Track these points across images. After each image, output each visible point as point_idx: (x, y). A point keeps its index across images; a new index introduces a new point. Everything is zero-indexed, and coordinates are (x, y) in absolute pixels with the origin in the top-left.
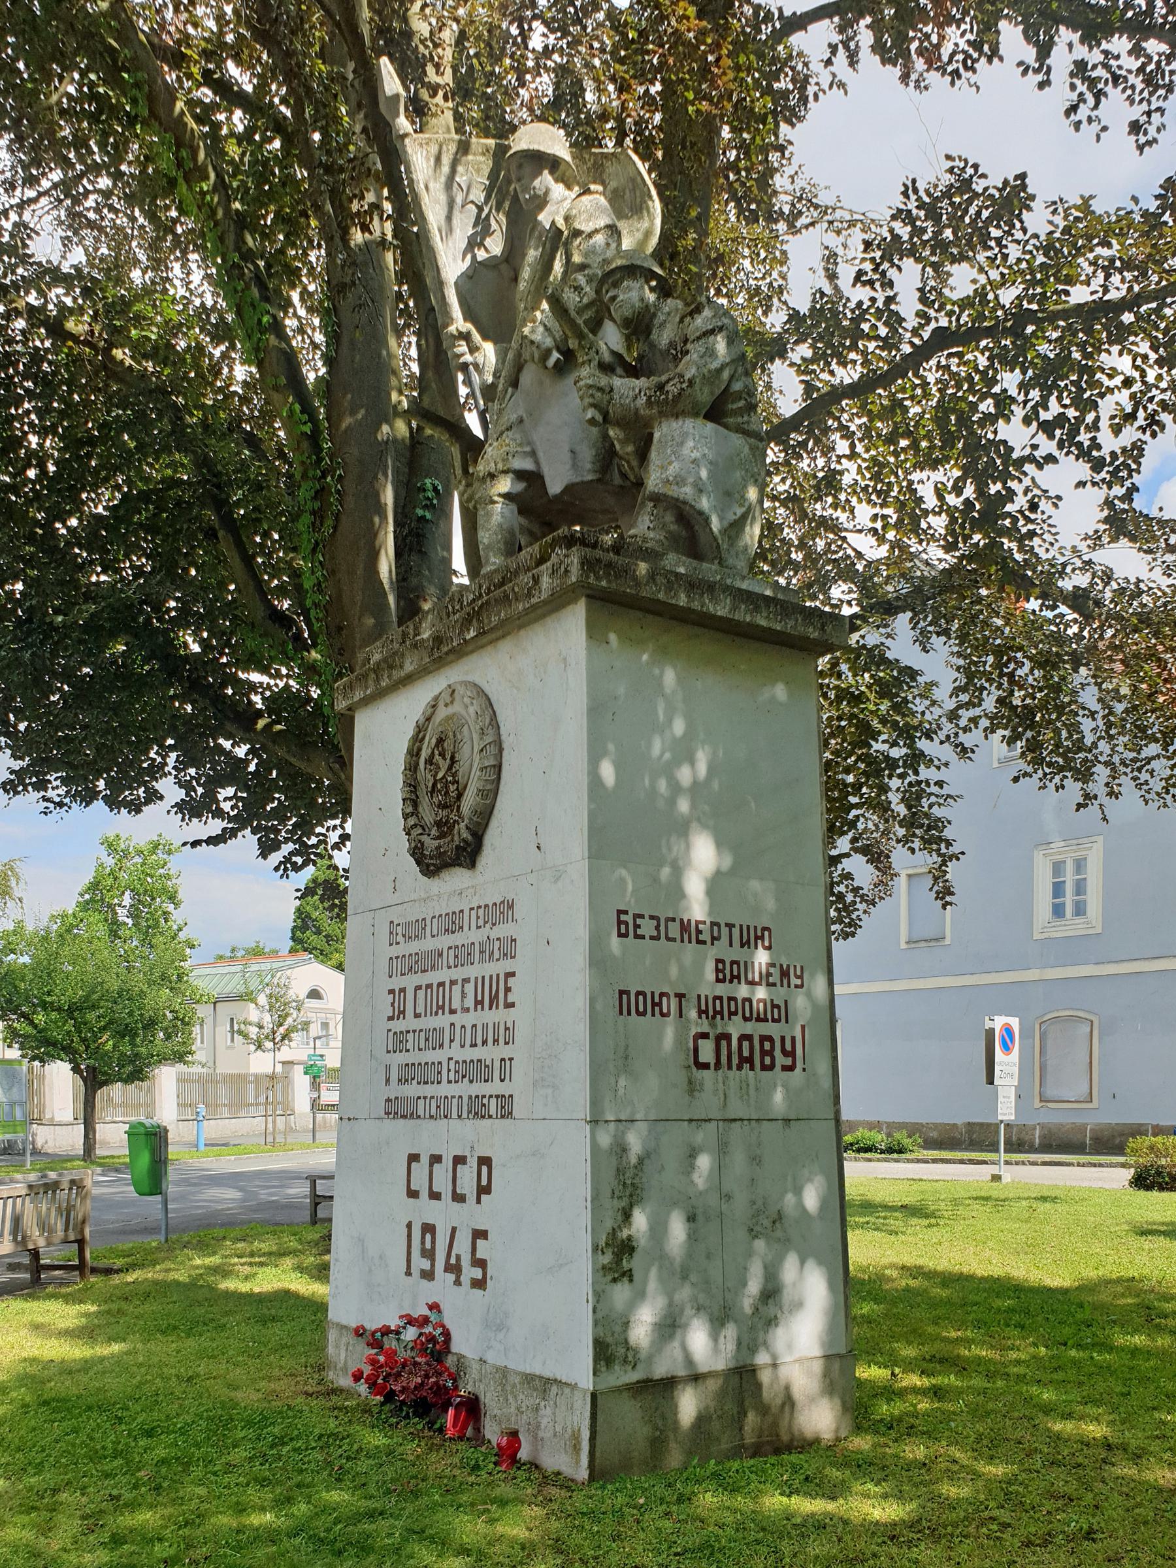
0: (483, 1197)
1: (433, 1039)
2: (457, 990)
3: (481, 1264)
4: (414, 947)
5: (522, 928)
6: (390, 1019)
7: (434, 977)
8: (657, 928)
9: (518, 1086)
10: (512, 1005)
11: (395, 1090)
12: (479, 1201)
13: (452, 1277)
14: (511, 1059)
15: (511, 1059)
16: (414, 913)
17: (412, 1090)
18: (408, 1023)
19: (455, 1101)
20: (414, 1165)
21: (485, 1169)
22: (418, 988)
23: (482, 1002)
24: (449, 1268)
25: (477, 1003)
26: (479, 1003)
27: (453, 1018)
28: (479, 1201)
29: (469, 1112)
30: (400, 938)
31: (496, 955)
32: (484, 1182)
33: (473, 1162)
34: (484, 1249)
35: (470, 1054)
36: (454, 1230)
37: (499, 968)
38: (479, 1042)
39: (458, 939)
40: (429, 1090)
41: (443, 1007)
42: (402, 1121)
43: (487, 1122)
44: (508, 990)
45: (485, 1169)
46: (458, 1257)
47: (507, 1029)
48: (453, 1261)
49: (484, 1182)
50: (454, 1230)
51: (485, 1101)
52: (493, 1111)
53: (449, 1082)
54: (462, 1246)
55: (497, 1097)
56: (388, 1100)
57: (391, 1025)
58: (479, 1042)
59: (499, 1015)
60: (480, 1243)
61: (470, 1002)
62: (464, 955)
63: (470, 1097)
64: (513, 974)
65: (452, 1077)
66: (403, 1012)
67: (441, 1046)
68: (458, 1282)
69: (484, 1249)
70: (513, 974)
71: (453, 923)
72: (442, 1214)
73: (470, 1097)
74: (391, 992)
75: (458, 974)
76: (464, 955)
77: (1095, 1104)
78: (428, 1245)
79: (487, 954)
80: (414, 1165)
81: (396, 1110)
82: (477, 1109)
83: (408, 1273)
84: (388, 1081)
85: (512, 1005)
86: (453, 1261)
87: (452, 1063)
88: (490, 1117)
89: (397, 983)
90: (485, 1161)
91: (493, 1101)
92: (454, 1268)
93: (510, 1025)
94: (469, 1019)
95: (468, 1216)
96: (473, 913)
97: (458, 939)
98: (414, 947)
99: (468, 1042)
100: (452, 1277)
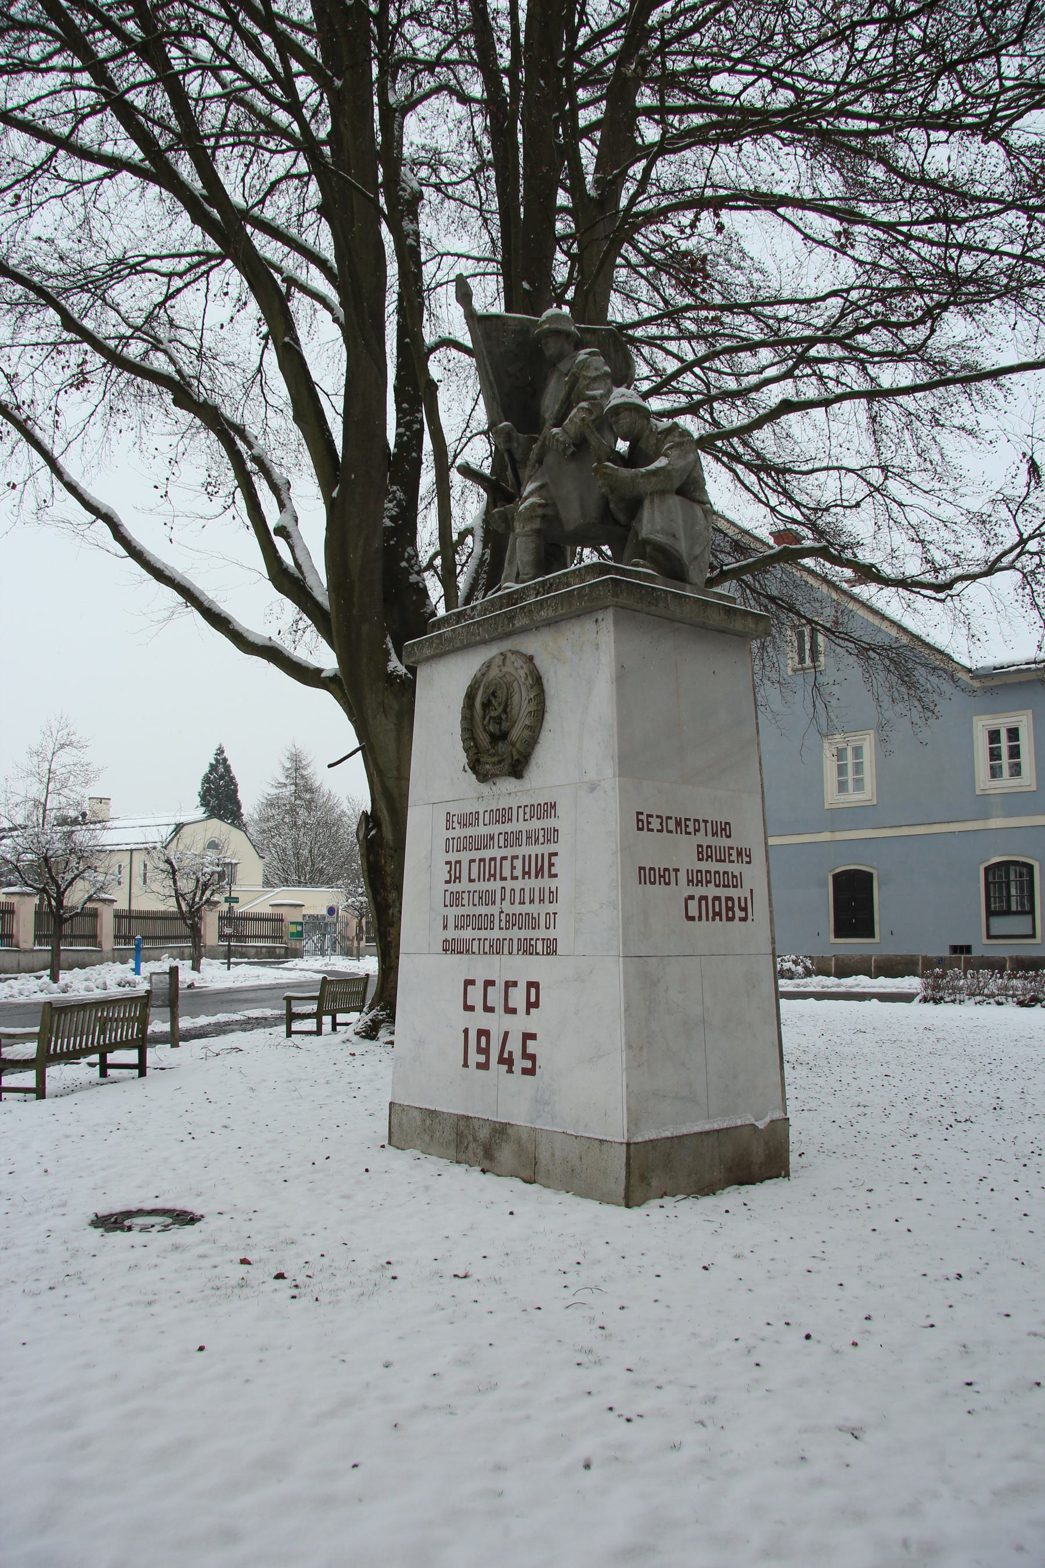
0: (532, 1010)
1: (485, 897)
2: (507, 864)
3: (532, 1058)
4: (470, 831)
5: (562, 822)
6: (447, 882)
7: (487, 854)
8: (661, 824)
9: (560, 932)
10: (556, 876)
11: (451, 934)
12: (528, 1013)
13: (506, 1067)
14: (555, 914)
15: (555, 914)
17: (468, 934)
18: (464, 885)
19: (506, 943)
21: (533, 991)
22: (472, 861)
23: (529, 873)
24: (501, 1061)
25: (524, 873)
26: (526, 873)
27: (503, 883)
28: (528, 1013)
29: (519, 950)
30: (456, 825)
31: (541, 840)
32: (533, 999)
33: (522, 986)
34: (532, 1047)
35: (518, 909)
36: (506, 1034)
37: (546, 849)
38: (527, 900)
39: (508, 827)
40: (483, 934)
41: (494, 876)
42: (460, 955)
43: (534, 957)
44: (551, 865)
45: (533, 991)
46: (510, 1053)
47: (551, 892)
48: (506, 1055)
49: (533, 999)
50: (506, 1034)
52: (539, 949)
53: (501, 929)
54: (514, 1045)
55: (543, 940)
56: (446, 941)
57: (448, 886)
58: (527, 900)
59: (545, 882)
60: (529, 1042)
61: (518, 872)
62: (512, 839)
63: (519, 939)
64: (556, 854)
65: (503, 925)
66: (459, 878)
67: (494, 903)
68: (510, 1071)
69: (532, 1047)
70: (556, 854)
71: (503, 816)
72: (496, 1023)
73: (519, 939)
74: (447, 863)
75: (509, 852)
76: (512, 839)
77: (1038, 940)
78: (483, 1044)
79: (532, 838)
80: (470, 987)
81: (450, 947)
82: (527, 948)
83: (466, 1065)
84: (445, 927)
85: (556, 876)
86: (506, 1055)
87: (503, 916)
88: (537, 954)
89: (453, 857)
90: (533, 985)
91: (540, 943)
92: (507, 1061)
93: (553, 889)
94: (517, 885)
95: (518, 1024)
96: (521, 811)
97: (508, 827)
98: (470, 831)
99: (517, 900)
100: (506, 1067)
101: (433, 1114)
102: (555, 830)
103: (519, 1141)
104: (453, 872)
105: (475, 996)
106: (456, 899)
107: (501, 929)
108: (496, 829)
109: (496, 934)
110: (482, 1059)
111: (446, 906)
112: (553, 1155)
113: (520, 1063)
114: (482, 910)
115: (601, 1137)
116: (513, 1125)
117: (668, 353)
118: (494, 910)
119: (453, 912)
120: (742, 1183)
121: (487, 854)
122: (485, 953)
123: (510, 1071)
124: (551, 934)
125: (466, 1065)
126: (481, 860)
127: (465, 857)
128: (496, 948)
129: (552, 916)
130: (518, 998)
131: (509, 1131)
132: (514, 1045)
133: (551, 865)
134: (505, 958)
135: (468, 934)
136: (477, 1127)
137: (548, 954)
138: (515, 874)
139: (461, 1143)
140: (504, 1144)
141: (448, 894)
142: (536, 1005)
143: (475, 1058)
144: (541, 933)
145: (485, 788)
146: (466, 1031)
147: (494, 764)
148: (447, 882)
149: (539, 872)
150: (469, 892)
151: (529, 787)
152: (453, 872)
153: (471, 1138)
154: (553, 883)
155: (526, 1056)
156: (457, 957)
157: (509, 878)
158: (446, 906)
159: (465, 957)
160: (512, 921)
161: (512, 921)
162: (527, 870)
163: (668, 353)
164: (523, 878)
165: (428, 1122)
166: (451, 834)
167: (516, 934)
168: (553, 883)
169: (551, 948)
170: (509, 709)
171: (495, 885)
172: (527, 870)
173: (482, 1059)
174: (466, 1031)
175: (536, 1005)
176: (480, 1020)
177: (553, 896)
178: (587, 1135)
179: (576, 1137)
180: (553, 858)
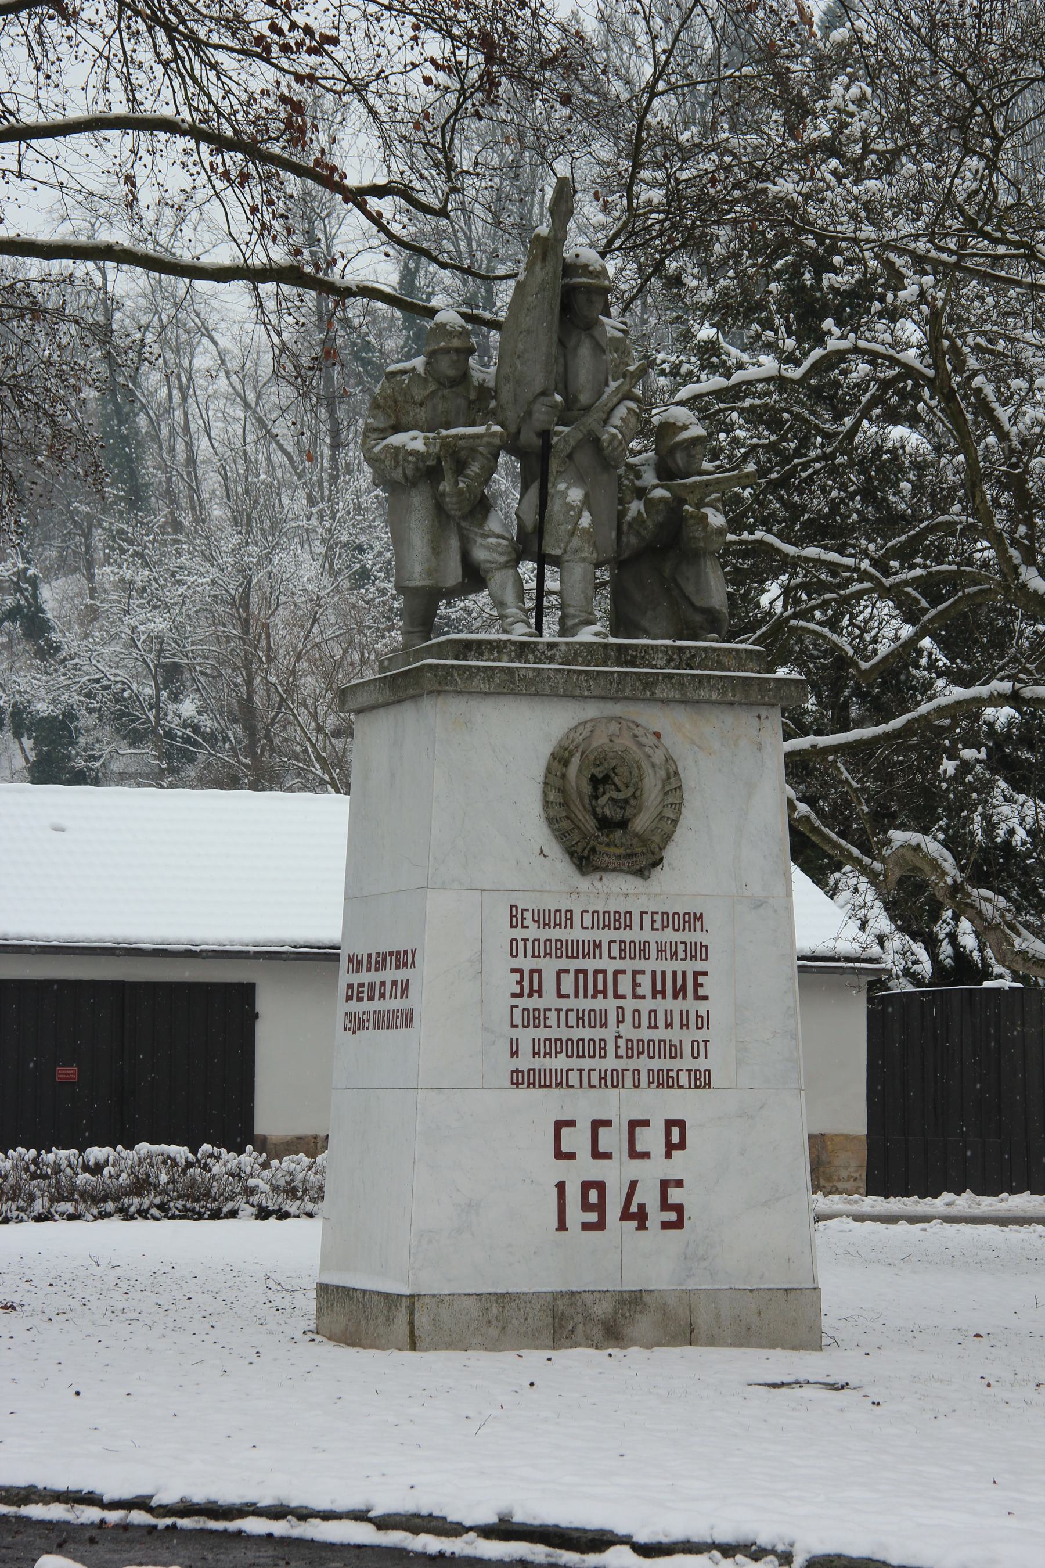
3: (679, 1209)
4: (555, 934)
5: (714, 935)
6: (514, 995)
7: (590, 965)
9: (715, 1062)
11: (525, 1061)
12: (668, 1155)
13: (635, 1223)
14: (706, 1042)
15: (706, 1042)
16: (551, 904)
17: (560, 1062)
20: (565, 1131)
24: (626, 1216)
27: (620, 1002)
28: (668, 1155)
29: (649, 1083)
30: (528, 922)
31: (681, 955)
36: (633, 1185)
37: (691, 967)
39: (626, 935)
40: (587, 1063)
44: (697, 985)
46: (642, 1207)
47: (698, 1016)
48: (634, 1209)
50: (633, 1185)
51: (674, 1074)
54: (648, 1196)
55: (689, 1071)
57: (516, 1001)
59: (690, 1004)
67: (605, 1025)
69: (675, 1196)
71: (620, 920)
75: (628, 965)
80: (565, 1131)
82: (665, 1081)
83: (562, 1226)
84: (515, 1053)
86: (634, 1209)
87: (621, 1043)
88: (680, 1087)
89: (527, 964)
94: (646, 1006)
97: (626, 935)
98: (555, 934)
101: (503, 1299)
102: (702, 946)
103: (663, 1309)
104: (526, 983)
105: (577, 1140)
106: (535, 1019)
107: (617, 1057)
108: (604, 936)
109: (610, 1062)
110: (593, 1217)
111: (513, 1026)
112: (718, 1316)
113: (656, 1216)
114: (586, 1033)
115: (786, 1286)
116: (651, 1291)
117: (340, 66)
118: (609, 1034)
119: (526, 1037)
120: (349, 1345)
121: (590, 965)
122: (591, 1087)
123: (642, 1227)
124: (701, 1064)
125: (562, 1226)
126: (577, 972)
127: (549, 967)
128: (613, 1080)
129: (702, 1045)
130: (651, 1139)
131: (647, 1298)
132: (648, 1196)
133: (697, 985)
134: (627, 1093)
135: (560, 1062)
136: (589, 1303)
137: (697, 1087)
138: (639, 991)
139: (561, 1326)
140: (638, 1317)
141: (518, 1012)
142: (682, 1146)
143: (575, 1215)
144: (686, 1062)
145: (584, 884)
146: (561, 1186)
147: (619, 857)
148: (514, 995)
149: (679, 992)
150: (559, 1010)
151: (657, 890)
152: (526, 983)
153: (579, 1318)
154: (702, 1007)
155: (665, 1206)
156: (538, 1093)
157: (630, 995)
158: (513, 1026)
159: (555, 1092)
160: (635, 1049)
161: (635, 1049)
162: (659, 987)
163: (340, 66)
164: (654, 997)
165: (495, 1311)
166: (519, 933)
167: (644, 1063)
168: (702, 1007)
169: (702, 1080)
170: (638, 793)
171: (599, 1003)
172: (659, 987)
173: (593, 1217)
174: (561, 1186)
175: (682, 1146)
176: (586, 1168)
177: (702, 1021)
178: (766, 1286)
179: (751, 1291)
180: (701, 979)
